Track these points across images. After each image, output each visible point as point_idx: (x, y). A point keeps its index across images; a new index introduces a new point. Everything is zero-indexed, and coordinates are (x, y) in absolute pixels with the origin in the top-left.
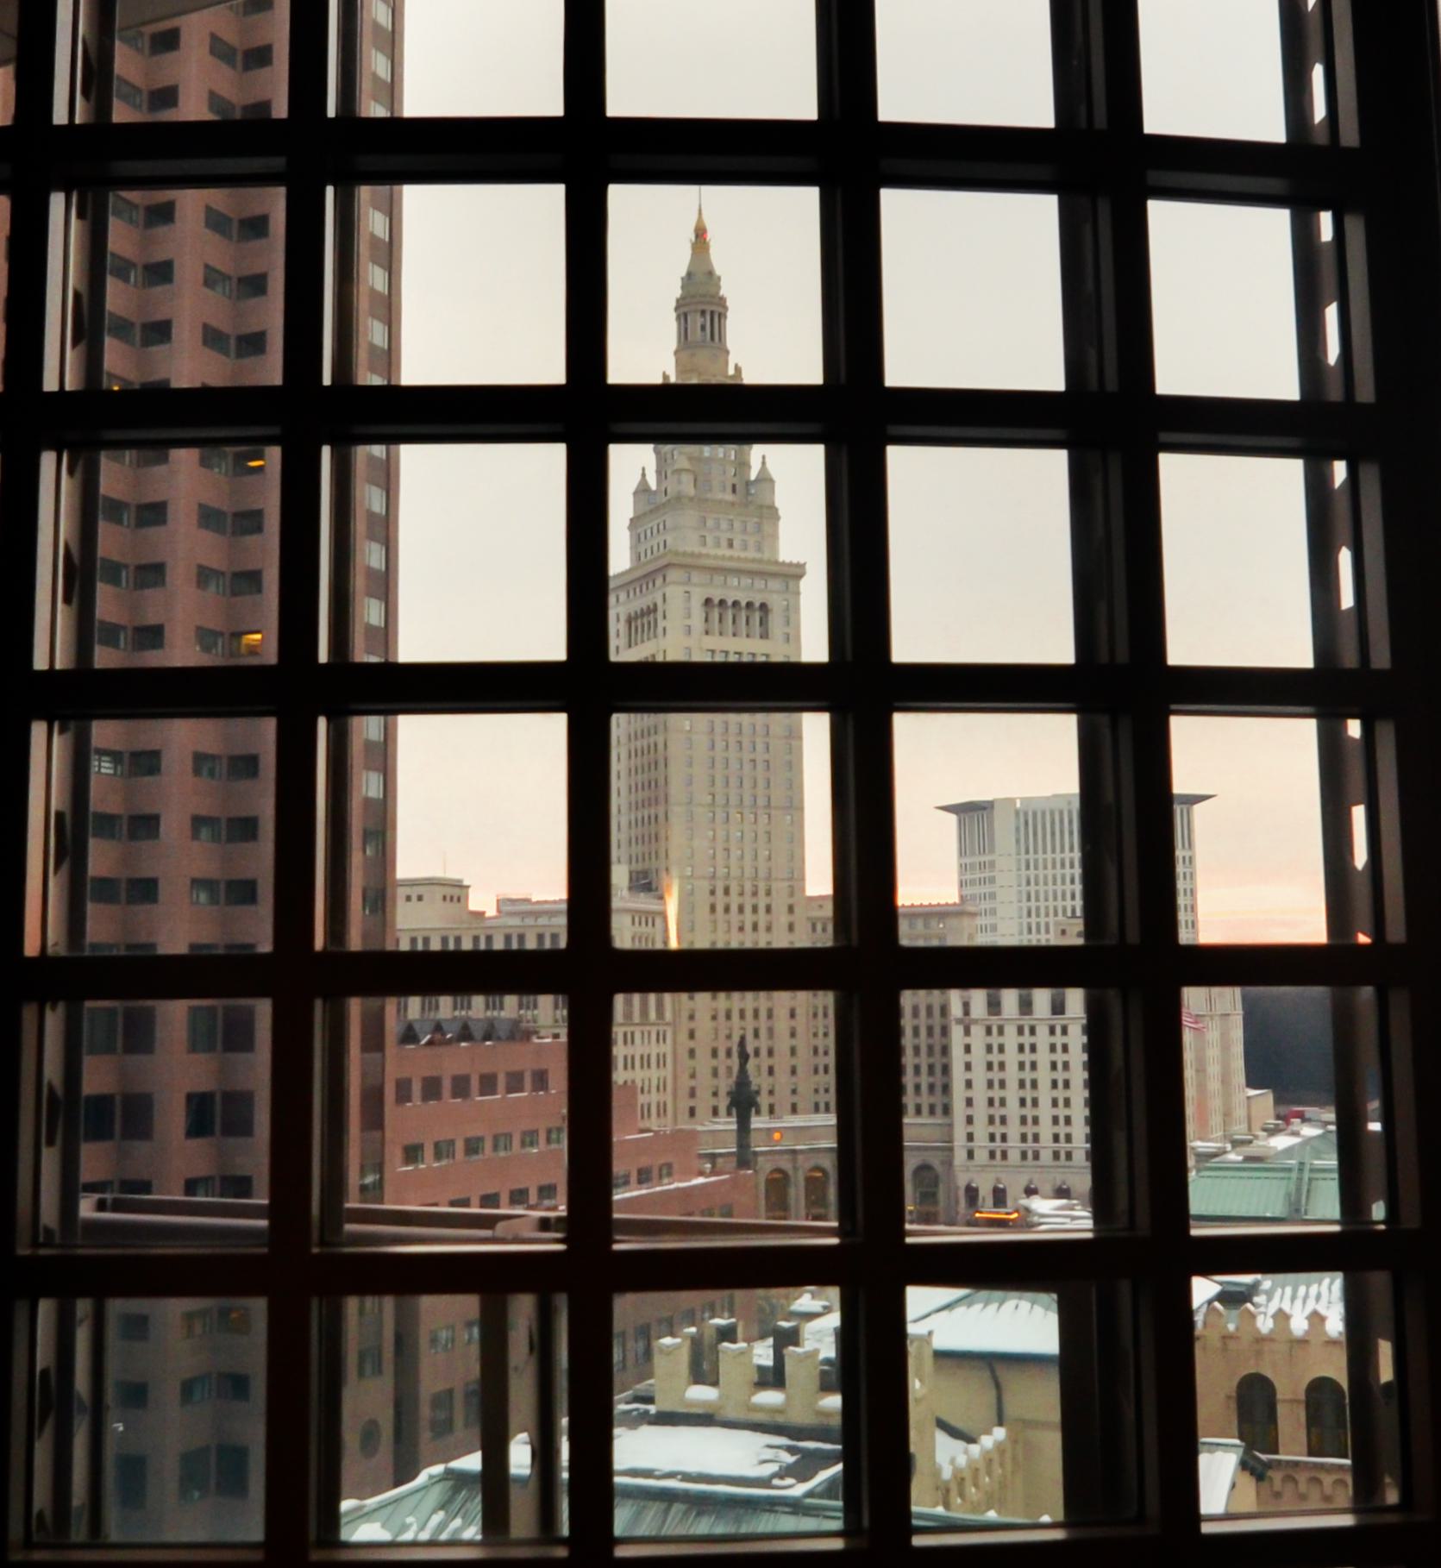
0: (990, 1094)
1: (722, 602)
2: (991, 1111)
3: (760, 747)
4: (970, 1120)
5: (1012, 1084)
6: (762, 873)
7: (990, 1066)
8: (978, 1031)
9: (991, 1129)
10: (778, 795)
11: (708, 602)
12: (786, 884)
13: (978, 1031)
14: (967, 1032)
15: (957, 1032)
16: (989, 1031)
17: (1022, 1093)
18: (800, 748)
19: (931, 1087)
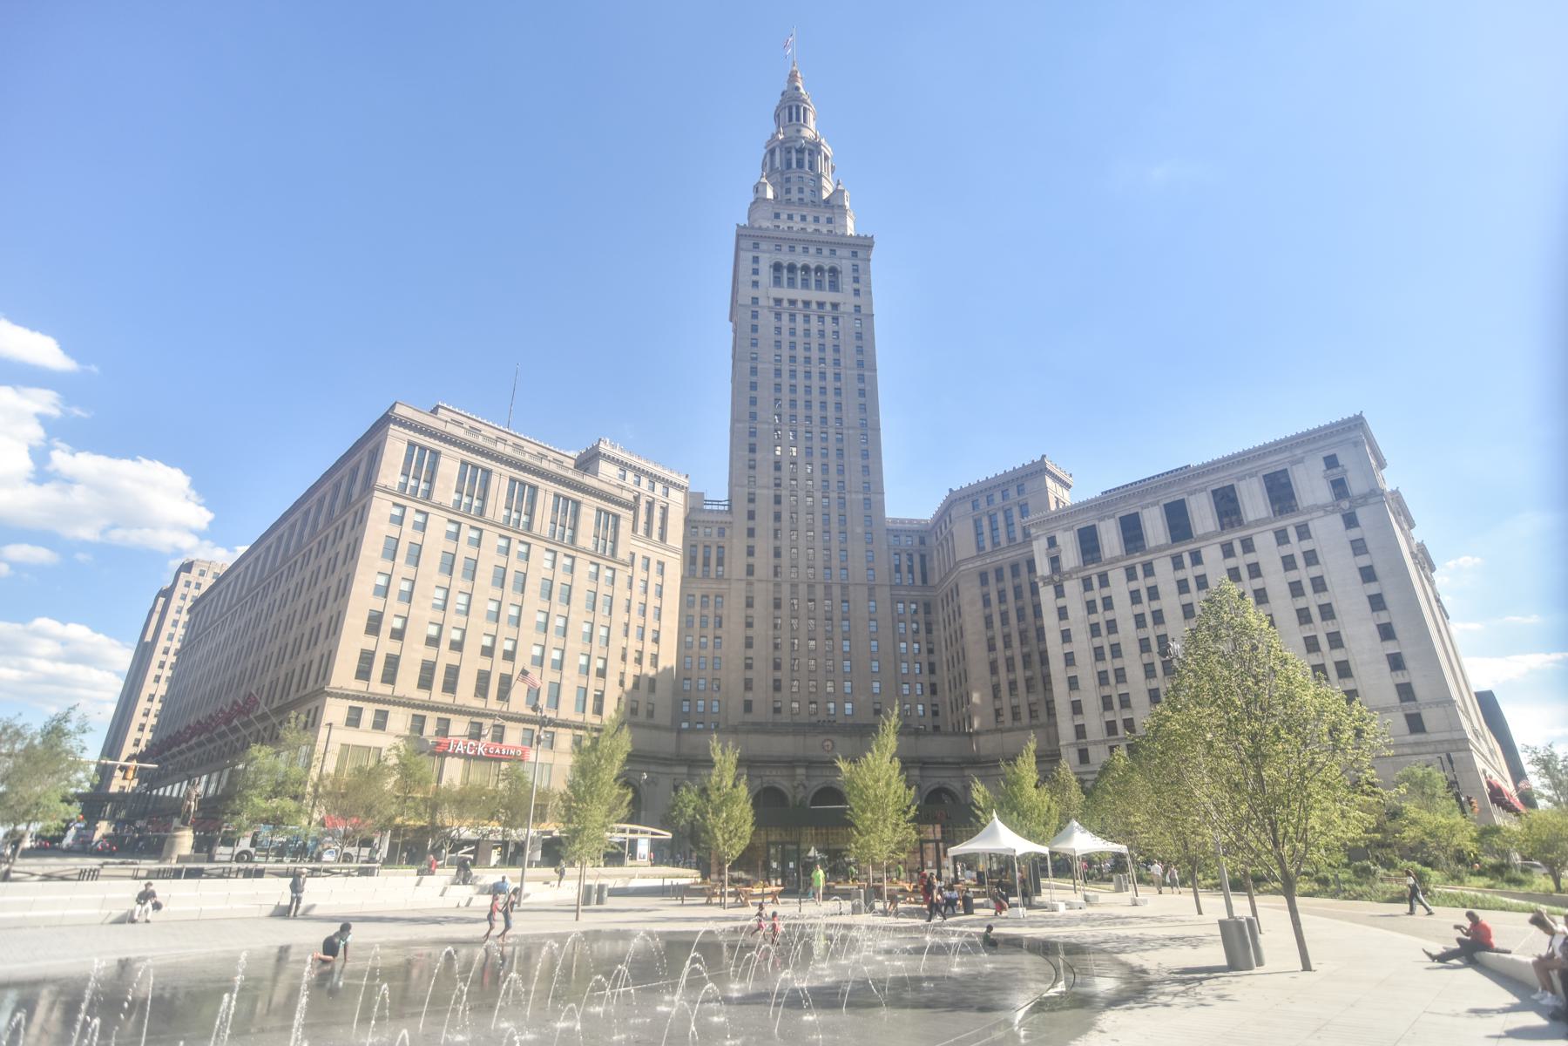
0: (1101, 667)
1: (792, 268)
2: (1107, 691)
3: (830, 376)
4: (1077, 708)
5: (1131, 649)
6: (834, 484)
7: (1095, 630)
8: (1072, 587)
9: (1109, 716)
10: (851, 416)
11: (777, 267)
12: (861, 496)
13: (1072, 587)
14: (1060, 592)
15: (1047, 594)
16: (1087, 585)
17: (1146, 658)
18: (875, 378)
19: (1028, 681)
